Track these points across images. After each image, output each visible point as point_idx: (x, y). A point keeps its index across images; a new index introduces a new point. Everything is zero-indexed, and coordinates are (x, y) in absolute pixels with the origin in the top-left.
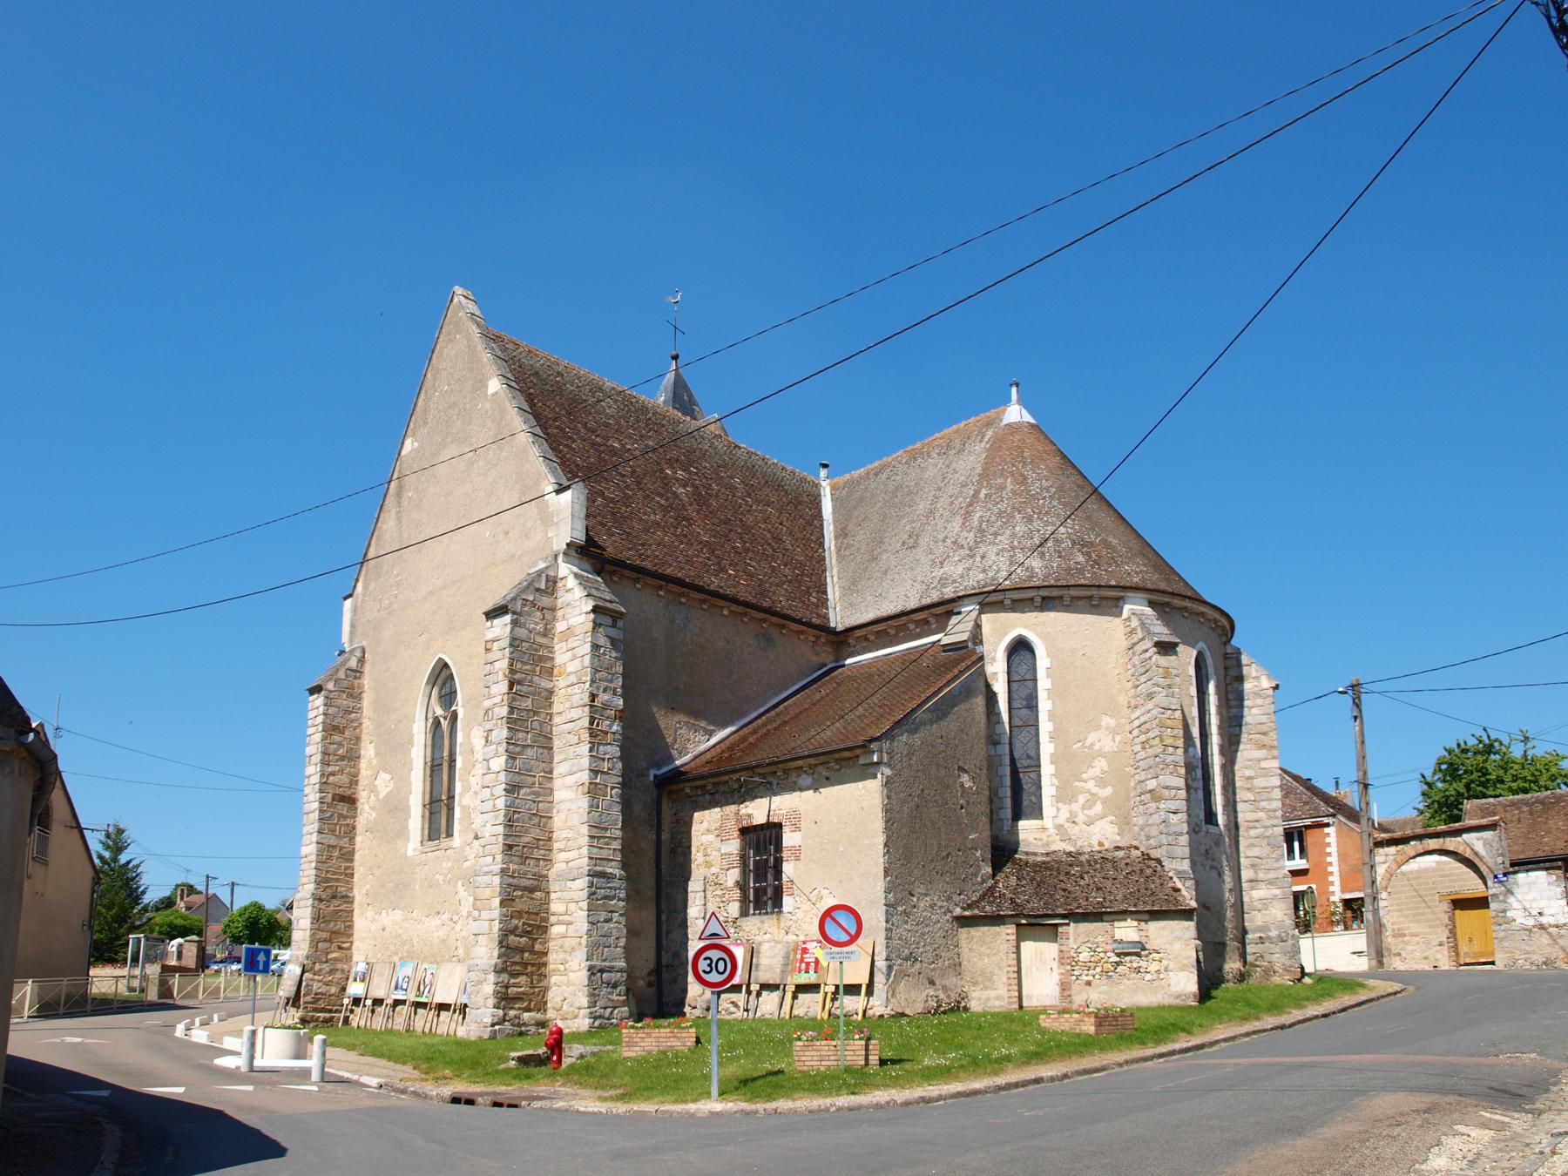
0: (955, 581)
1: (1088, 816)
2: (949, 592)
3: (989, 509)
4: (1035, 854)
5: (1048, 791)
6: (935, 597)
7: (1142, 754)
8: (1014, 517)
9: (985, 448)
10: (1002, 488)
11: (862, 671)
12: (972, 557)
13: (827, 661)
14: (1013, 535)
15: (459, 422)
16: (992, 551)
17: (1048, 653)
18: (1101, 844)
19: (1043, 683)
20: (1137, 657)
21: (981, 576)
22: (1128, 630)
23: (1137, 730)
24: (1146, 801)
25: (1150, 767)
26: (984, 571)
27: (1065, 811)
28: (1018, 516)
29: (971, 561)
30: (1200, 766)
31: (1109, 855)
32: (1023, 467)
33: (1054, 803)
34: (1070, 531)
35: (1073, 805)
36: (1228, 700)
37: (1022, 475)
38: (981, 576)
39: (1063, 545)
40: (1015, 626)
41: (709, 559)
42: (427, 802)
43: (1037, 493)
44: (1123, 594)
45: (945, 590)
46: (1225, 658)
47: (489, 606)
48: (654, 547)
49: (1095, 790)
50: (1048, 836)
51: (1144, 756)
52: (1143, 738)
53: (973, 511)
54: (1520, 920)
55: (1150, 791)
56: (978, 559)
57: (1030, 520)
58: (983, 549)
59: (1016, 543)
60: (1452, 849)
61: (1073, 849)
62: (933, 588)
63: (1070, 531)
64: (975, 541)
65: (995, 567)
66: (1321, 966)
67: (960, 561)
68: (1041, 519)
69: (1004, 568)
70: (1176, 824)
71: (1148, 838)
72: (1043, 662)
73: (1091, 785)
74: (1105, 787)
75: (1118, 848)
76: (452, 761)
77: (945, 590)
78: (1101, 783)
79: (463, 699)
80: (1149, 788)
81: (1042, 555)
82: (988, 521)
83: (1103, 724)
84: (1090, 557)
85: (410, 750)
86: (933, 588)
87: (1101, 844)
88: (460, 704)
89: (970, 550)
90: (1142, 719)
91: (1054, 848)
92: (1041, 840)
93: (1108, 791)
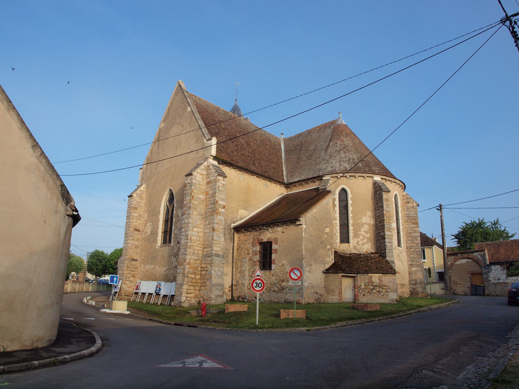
0: (323, 170)
1: (363, 243)
2: (321, 173)
3: (333, 149)
4: (347, 254)
5: (351, 235)
6: (317, 174)
7: (379, 225)
8: (340, 152)
9: (331, 131)
10: (336, 143)
11: (294, 196)
12: (328, 163)
13: (284, 192)
14: (340, 157)
15: (178, 119)
16: (334, 162)
17: (351, 193)
18: (366, 252)
19: (350, 202)
20: (377, 195)
21: (331, 169)
22: (375, 187)
23: (377, 217)
24: (380, 239)
25: (382, 229)
26: (332, 167)
27: (356, 240)
28: (342, 152)
29: (328, 164)
30: (396, 229)
31: (369, 255)
32: (343, 137)
33: (352, 238)
34: (357, 156)
35: (358, 239)
36: (404, 209)
37: (343, 140)
38: (331, 169)
39: (355, 161)
40: (341, 185)
41: (250, 161)
42: (163, 232)
43: (347, 145)
44: (373, 176)
45: (320, 173)
46: (403, 196)
47: (186, 173)
48: (235, 157)
49: (365, 235)
50: (351, 249)
51: (380, 225)
52: (379, 219)
53: (328, 150)
54: (493, 281)
55: (382, 236)
56: (330, 164)
57: (345, 153)
58: (331, 161)
59: (341, 160)
60: (471, 257)
61: (357, 253)
62: (317, 172)
63: (357, 156)
64: (329, 158)
65: (335, 166)
66: (433, 292)
67: (324, 164)
68: (349, 153)
69: (338, 167)
70: (389, 247)
71: (381, 251)
72: (350, 196)
73: (363, 233)
74: (368, 234)
75: (372, 253)
76: (172, 219)
77: (320, 173)
78: (366, 232)
79: (176, 200)
80: (381, 235)
81: (349, 163)
82: (332, 153)
83: (367, 214)
84: (363, 164)
85: (159, 215)
86: (317, 172)
87: (366, 252)
88: (175, 202)
89: (327, 161)
90: (379, 214)
91: (352, 252)
92: (348, 250)
93: (368, 235)
